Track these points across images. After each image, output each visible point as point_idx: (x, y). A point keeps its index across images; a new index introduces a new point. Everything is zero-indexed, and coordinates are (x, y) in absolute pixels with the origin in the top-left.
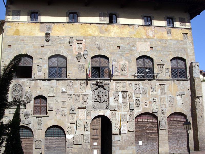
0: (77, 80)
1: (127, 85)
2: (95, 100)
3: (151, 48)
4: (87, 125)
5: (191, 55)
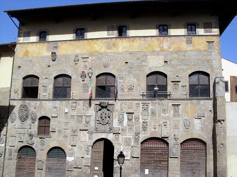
1: (134, 106)
2: (99, 122)
3: (165, 62)
4: (88, 148)
5: (216, 69)
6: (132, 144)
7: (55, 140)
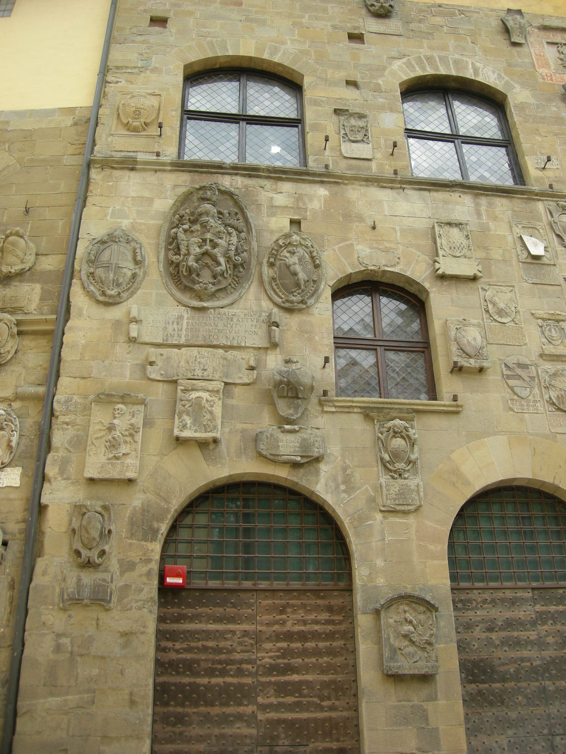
7: (494, 434)
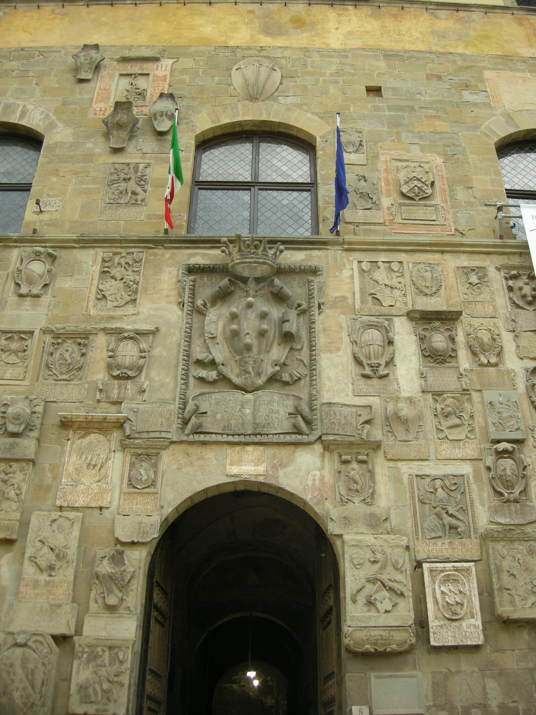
0: (86, 242)
1: (451, 278)
4: (117, 558)
6: (483, 516)
